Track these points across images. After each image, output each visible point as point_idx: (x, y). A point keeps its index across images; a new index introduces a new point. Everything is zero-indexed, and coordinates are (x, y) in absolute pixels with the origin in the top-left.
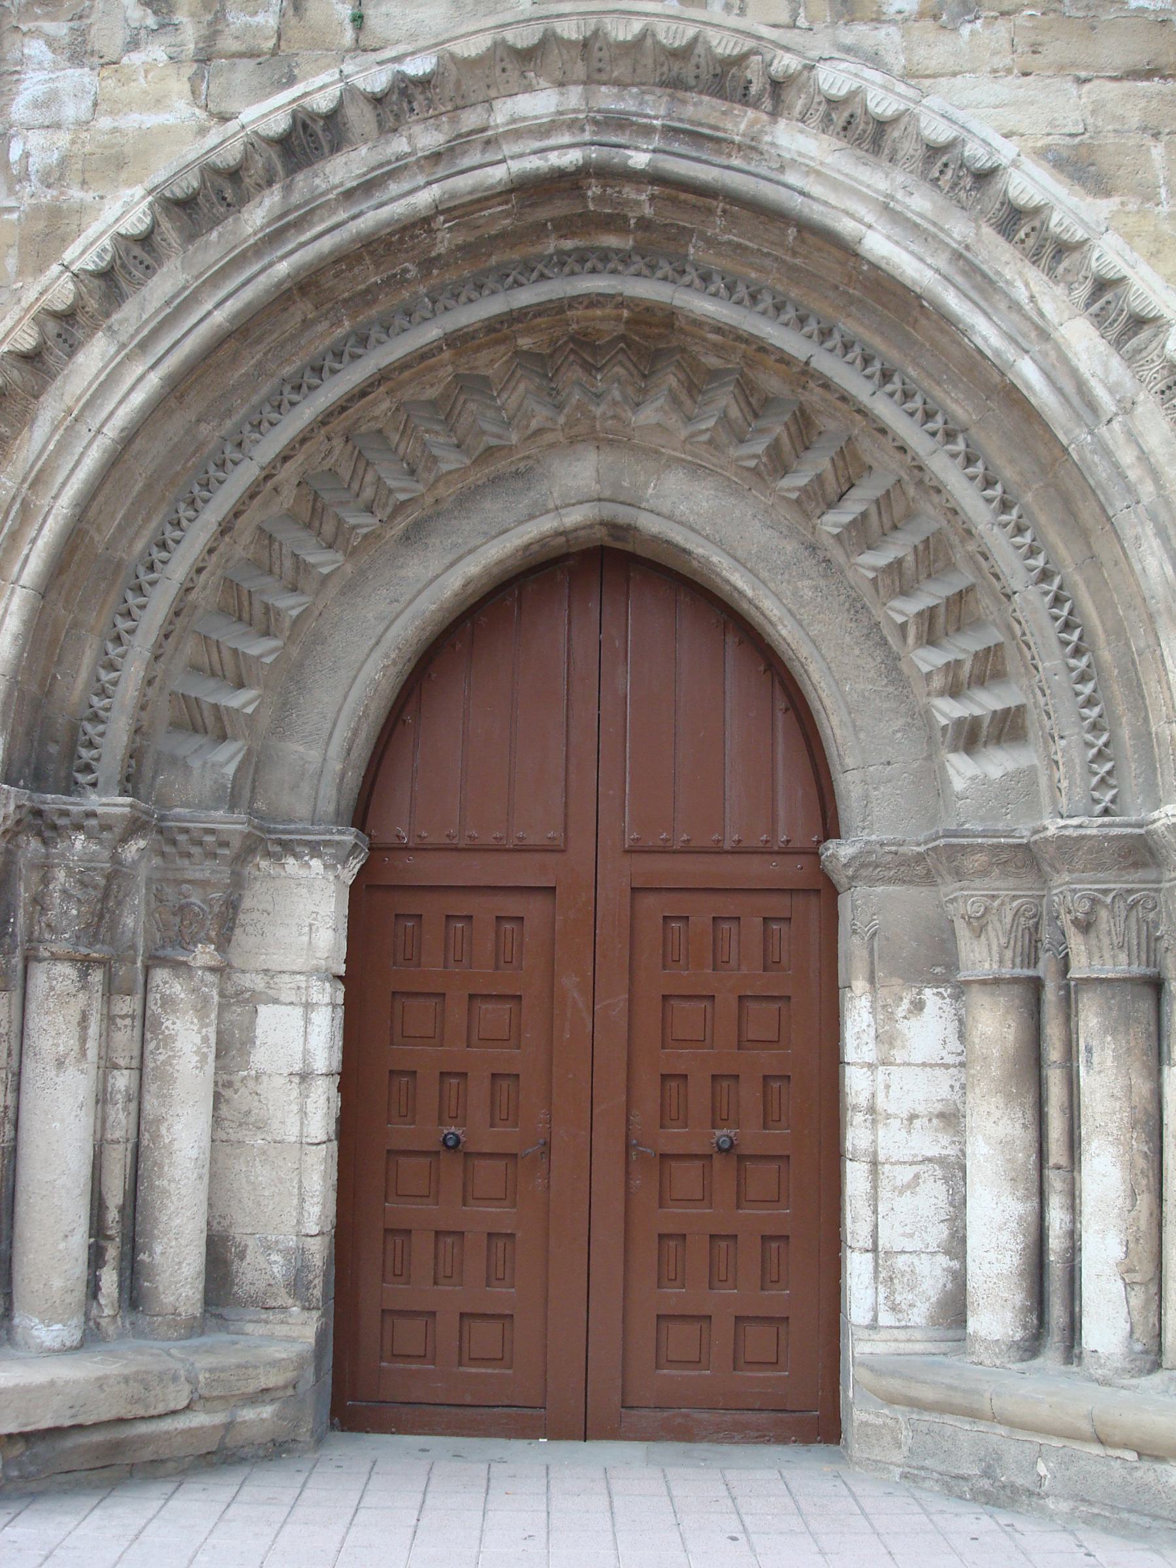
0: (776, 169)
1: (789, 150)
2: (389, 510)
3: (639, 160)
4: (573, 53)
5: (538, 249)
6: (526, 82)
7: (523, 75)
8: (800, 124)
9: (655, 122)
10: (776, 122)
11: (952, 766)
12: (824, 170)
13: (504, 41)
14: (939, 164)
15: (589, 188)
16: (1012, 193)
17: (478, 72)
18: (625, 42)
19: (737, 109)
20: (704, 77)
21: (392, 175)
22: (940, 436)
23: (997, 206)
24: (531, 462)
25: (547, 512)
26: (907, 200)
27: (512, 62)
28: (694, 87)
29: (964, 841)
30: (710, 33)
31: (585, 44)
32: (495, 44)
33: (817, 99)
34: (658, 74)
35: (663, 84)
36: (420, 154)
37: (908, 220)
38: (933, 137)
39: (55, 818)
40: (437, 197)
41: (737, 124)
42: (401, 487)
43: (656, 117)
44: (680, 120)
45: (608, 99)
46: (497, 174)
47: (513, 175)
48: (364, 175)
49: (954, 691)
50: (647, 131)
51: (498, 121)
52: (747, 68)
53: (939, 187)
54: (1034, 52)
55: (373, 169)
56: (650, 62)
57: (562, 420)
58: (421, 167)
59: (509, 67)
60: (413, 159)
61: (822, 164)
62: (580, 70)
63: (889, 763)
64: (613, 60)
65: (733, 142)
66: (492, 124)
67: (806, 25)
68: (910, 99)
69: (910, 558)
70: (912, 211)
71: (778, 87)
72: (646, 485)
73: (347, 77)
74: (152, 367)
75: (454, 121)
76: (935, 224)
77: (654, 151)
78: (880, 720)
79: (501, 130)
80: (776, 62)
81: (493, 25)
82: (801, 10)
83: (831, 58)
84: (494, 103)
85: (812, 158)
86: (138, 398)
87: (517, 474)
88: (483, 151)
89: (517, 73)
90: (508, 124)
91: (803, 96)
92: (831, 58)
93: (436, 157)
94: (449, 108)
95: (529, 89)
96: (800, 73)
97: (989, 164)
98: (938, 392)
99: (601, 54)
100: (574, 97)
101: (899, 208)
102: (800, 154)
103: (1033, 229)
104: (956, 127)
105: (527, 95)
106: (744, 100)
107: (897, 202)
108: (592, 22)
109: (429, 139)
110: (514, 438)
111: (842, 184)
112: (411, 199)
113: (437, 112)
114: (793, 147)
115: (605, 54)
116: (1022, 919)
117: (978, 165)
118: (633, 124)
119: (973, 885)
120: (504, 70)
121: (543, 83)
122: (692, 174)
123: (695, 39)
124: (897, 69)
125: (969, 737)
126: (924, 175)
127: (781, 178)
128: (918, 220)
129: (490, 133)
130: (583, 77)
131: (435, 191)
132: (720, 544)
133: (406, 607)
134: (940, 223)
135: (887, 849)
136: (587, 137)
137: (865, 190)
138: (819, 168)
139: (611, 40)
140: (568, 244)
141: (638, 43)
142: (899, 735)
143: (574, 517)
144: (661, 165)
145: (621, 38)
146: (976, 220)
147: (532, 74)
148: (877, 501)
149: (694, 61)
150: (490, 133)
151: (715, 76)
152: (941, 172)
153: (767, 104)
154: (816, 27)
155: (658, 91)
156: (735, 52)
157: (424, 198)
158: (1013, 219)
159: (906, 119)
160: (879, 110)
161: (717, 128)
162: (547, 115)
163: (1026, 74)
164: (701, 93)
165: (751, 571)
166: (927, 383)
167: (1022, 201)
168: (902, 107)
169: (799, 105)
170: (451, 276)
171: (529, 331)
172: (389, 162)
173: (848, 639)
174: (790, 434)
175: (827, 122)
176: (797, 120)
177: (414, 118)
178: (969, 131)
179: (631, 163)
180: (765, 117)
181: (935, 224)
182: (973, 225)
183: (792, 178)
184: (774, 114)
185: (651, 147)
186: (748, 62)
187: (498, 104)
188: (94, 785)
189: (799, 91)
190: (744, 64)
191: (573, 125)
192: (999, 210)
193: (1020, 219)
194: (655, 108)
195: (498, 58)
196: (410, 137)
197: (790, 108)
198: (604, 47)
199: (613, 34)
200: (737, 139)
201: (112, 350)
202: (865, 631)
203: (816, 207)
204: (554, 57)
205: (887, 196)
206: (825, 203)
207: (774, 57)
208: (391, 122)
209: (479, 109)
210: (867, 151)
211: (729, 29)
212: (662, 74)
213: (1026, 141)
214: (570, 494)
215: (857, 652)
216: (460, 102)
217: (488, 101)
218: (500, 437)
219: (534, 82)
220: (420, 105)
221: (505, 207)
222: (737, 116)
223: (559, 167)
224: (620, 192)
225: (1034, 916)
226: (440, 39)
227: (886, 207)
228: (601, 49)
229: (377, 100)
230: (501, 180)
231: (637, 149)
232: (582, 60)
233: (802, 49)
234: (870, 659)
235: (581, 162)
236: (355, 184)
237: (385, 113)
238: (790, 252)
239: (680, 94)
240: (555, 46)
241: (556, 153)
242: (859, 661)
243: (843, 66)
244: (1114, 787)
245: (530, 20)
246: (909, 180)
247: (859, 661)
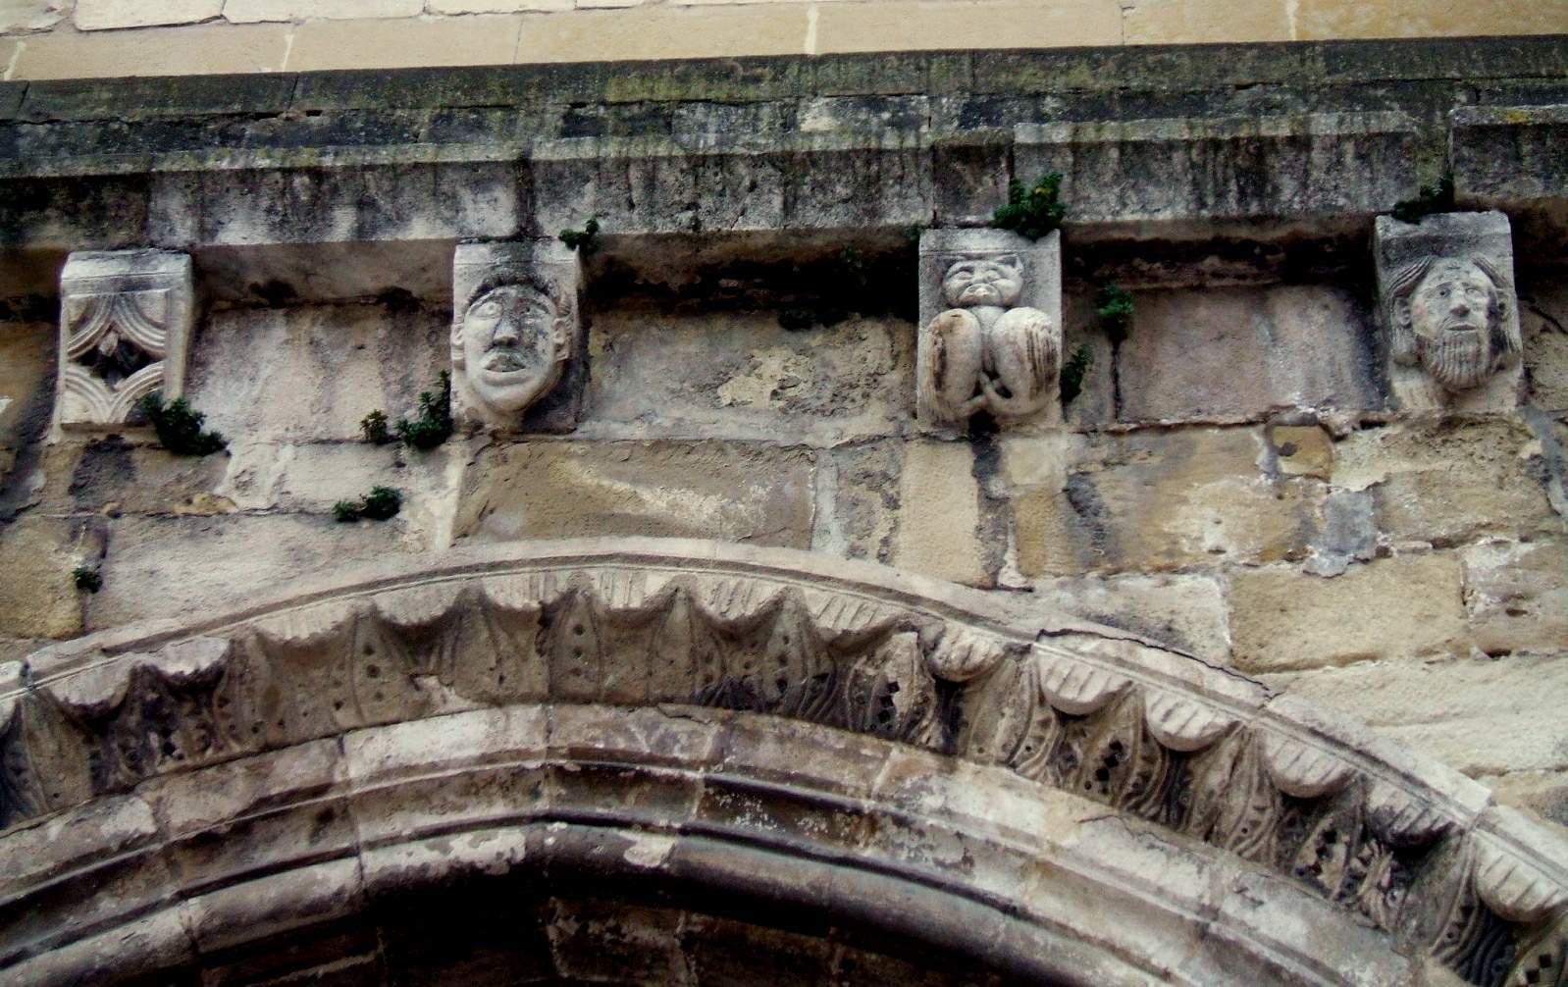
0: (955, 866)
1: (981, 824)
3: (649, 850)
4: (522, 638)
6: (417, 696)
7: (412, 679)
8: (1006, 771)
9: (690, 774)
10: (952, 770)
12: (1059, 862)
13: (375, 611)
14: (1315, 836)
15: (550, 916)
16: (1488, 880)
17: (317, 674)
18: (627, 611)
19: (869, 745)
20: (797, 683)
21: (105, 879)
23: (1455, 916)
26: (1249, 916)
27: (388, 655)
28: (777, 703)
30: (807, 592)
31: (546, 618)
32: (356, 620)
33: (1038, 716)
34: (699, 678)
35: (711, 699)
36: (174, 838)
37: (1252, 958)
38: (1293, 774)
40: (196, 923)
41: (866, 776)
43: (692, 765)
44: (746, 770)
45: (588, 727)
46: (336, 877)
47: (369, 880)
48: (46, 876)
50: (677, 790)
51: (353, 773)
52: (885, 659)
53: (1320, 887)
54: (1512, 613)
55: (68, 865)
56: (682, 658)
58: (172, 864)
59: (383, 664)
60: (157, 847)
61: (1054, 849)
62: (535, 673)
64: (605, 653)
65: (857, 812)
66: (338, 778)
67: (1018, 581)
68: (1239, 704)
70: (1261, 940)
71: (953, 694)
73: (37, 675)
75: (258, 773)
76: (1315, 965)
77: (684, 832)
79: (356, 791)
80: (945, 643)
81: (355, 582)
82: (1010, 557)
83: (1064, 633)
84: (348, 739)
85: (1031, 839)
88: (315, 836)
89: (398, 679)
90: (371, 779)
91: (1007, 711)
92: (1064, 633)
93: (206, 843)
94: (248, 748)
95: (422, 710)
96: (999, 663)
97: (1424, 825)
99: (578, 640)
100: (521, 729)
101: (1230, 934)
102: (1005, 831)
103: (1545, 961)
104: (1345, 753)
105: (419, 725)
106: (882, 726)
107: (1227, 920)
108: (563, 579)
109: (192, 807)
111: (1101, 888)
112: (138, 928)
113: (222, 754)
114: (990, 817)
115: (587, 640)
117: (1400, 827)
118: (642, 778)
120: (373, 672)
121: (455, 700)
122: (763, 875)
123: (777, 605)
124: (1217, 654)
126: (1284, 863)
127: (967, 882)
128: (1277, 959)
129: (331, 796)
130: (541, 687)
131: (194, 911)
134: (1328, 963)
136: (542, 806)
137: (1151, 899)
138: (1049, 857)
139: (600, 611)
144: (694, 858)
145: (618, 603)
146: (1410, 952)
147: (432, 681)
149: (775, 647)
150: (331, 796)
151: (821, 678)
152: (1322, 852)
153: (932, 731)
154: (1038, 584)
155: (698, 712)
156: (858, 626)
157: (167, 926)
159: (1231, 746)
160: (1171, 727)
161: (826, 785)
162: (461, 763)
163: (1495, 654)
164: (790, 714)
167: (1508, 897)
168: (1223, 721)
169: (1001, 730)
172: (103, 853)
175: (1063, 763)
176: (1000, 763)
177: (171, 764)
178: (1375, 760)
179: (633, 857)
180: (929, 760)
181: (1315, 965)
182: (1404, 962)
183: (987, 880)
184: (949, 752)
185: (677, 825)
186: (889, 647)
187: (353, 741)
189: (999, 702)
190: (880, 653)
191: (514, 782)
192: (1461, 926)
193: (1513, 942)
194: (693, 741)
195: (360, 644)
196: (157, 806)
197: (980, 738)
198: (587, 625)
199: (603, 598)
200: (868, 805)
203: (1039, 936)
204: (480, 649)
205: (1202, 910)
206: (1063, 929)
207: (942, 634)
208: (122, 774)
209: (315, 750)
210: (1154, 819)
211: (848, 584)
212: (708, 679)
213: (1508, 783)
216: (273, 735)
217: (337, 735)
219: (436, 697)
220: (187, 737)
221: (360, 960)
222: (868, 759)
223: (472, 866)
224: (616, 930)
226: (242, 608)
227: (1202, 934)
228: (579, 630)
229: (92, 724)
230: (339, 894)
231: (647, 827)
232: (541, 652)
233: (1001, 616)
235: (521, 855)
236: (21, 894)
237: (110, 751)
238: (63, 153)
239: (747, 719)
240: (481, 625)
241: (468, 837)
243: (1089, 646)
245: (435, 573)
246: (1253, 876)
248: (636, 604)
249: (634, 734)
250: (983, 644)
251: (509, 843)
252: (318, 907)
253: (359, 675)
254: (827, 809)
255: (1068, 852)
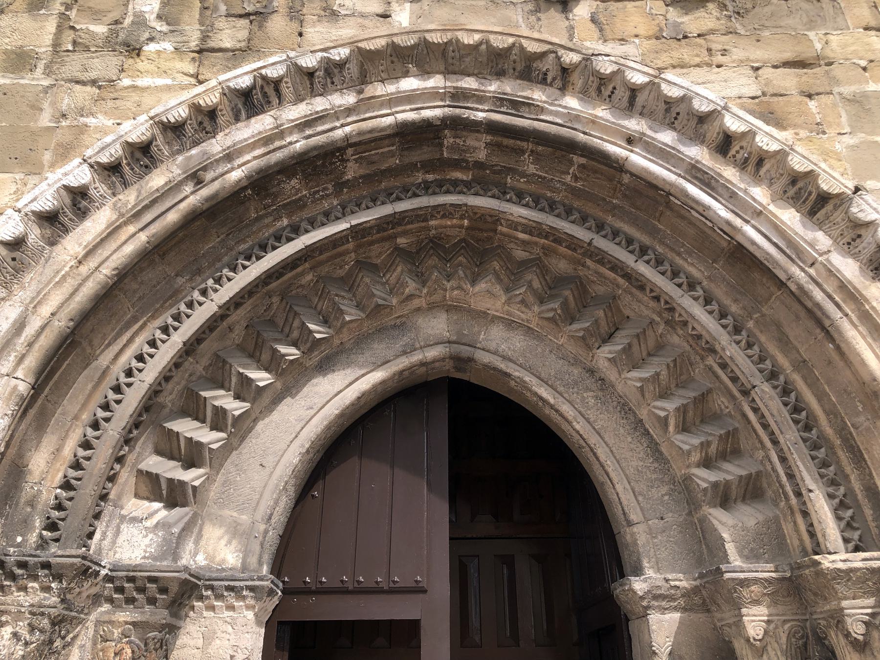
2: (309, 345)
5: (411, 180)
11: (715, 518)
18: (469, 45)
22: (685, 287)
24: (404, 319)
25: (415, 350)
29: (742, 576)
39: (15, 569)
42: (318, 331)
49: (707, 463)
57: (425, 291)
63: (662, 519)
68: (652, 75)
69: (664, 373)
72: (479, 333)
74: (142, 229)
78: (652, 487)
86: (129, 249)
87: (394, 327)
98: (679, 261)
103: (742, 148)
110: (394, 301)
112: (331, 134)
116: (793, 640)
119: (751, 612)
120: (392, 62)
123: (514, 44)
125: (724, 497)
132: (530, 370)
133: (317, 412)
135: (672, 583)
140: (430, 177)
141: (476, 47)
142: (666, 498)
143: (431, 354)
148: (638, 336)
153: (558, 83)
158: (725, 144)
161: (528, 98)
165: (551, 386)
166: (670, 255)
170: (355, 194)
171: (404, 234)
173: (622, 431)
174: (574, 296)
180: (558, 92)
188: (57, 540)
195: (389, 53)
201: (115, 217)
202: (633, 426)
214: (429, 341)
215: (629, 439)
218: (385, 300)
225: (802, 637)
228: (453, 52)
234: (639, 444)
242: (632, 446)
244: (858, 529)
247: (632, 446)
248: (471, 43)
249: (469, 83)
250: (575, 58)
251: (438, 112)
252: (383, 129)
253: (389, 63)
254: (529, 105)
255: (601, 118)
